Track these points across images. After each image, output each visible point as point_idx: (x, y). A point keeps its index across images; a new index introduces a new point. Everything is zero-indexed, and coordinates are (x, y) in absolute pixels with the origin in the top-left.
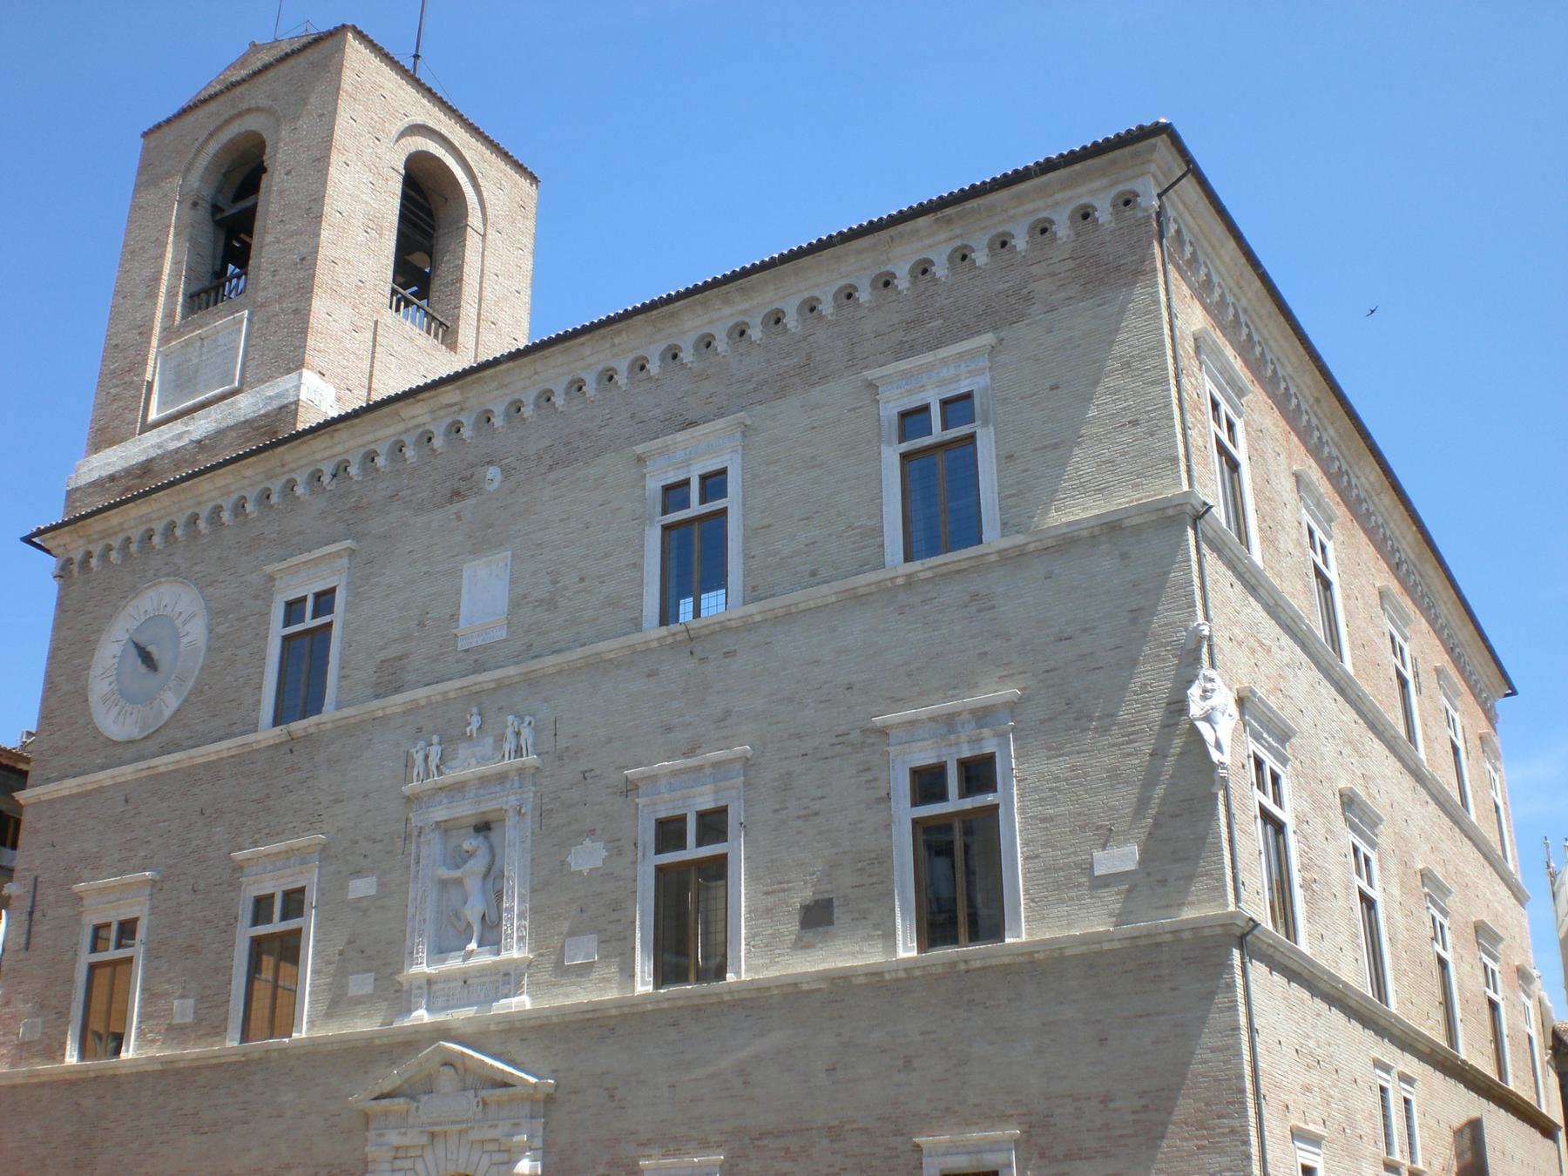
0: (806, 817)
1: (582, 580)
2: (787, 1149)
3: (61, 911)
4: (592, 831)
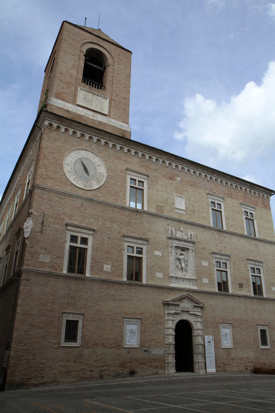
0: (238, 269)
1: (199, 211)
2: (240, 323)
3: (56, 226)
4: (205, 259)
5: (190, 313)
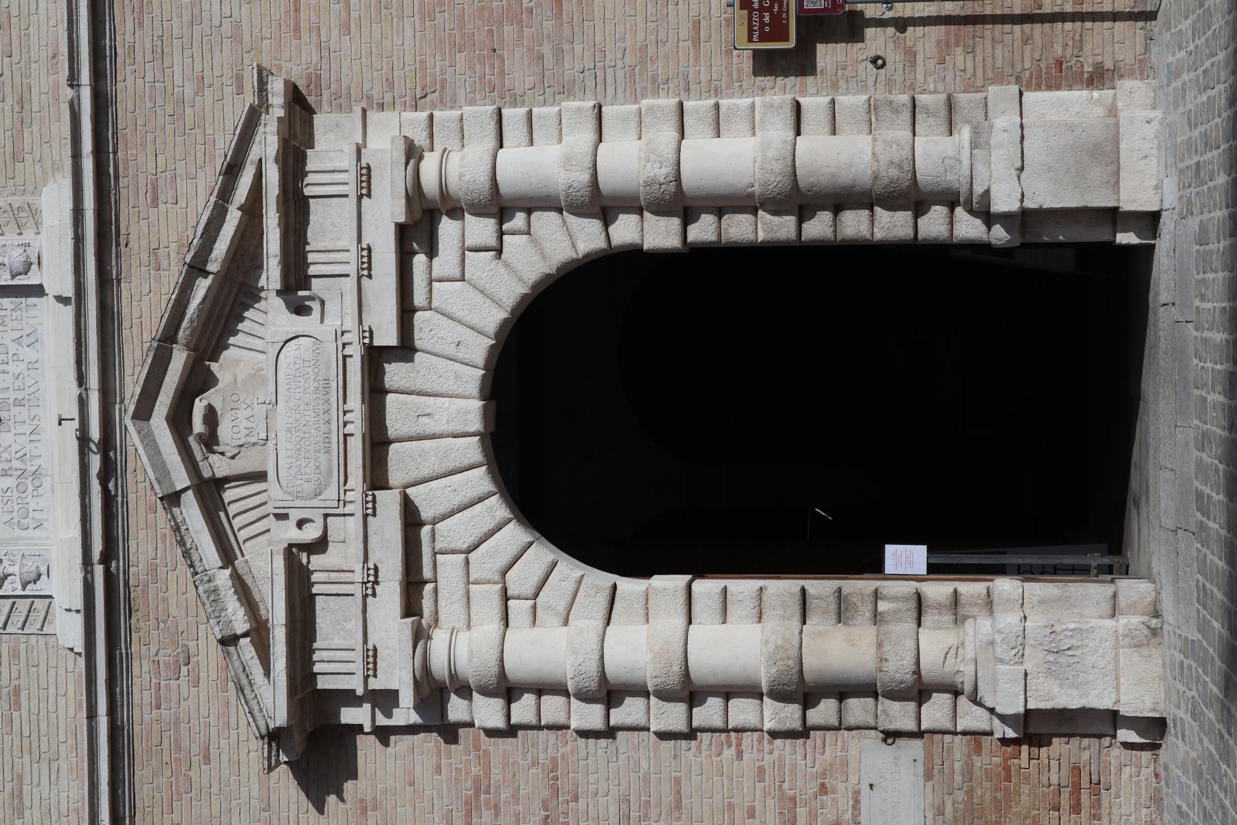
5: (387, 336)
